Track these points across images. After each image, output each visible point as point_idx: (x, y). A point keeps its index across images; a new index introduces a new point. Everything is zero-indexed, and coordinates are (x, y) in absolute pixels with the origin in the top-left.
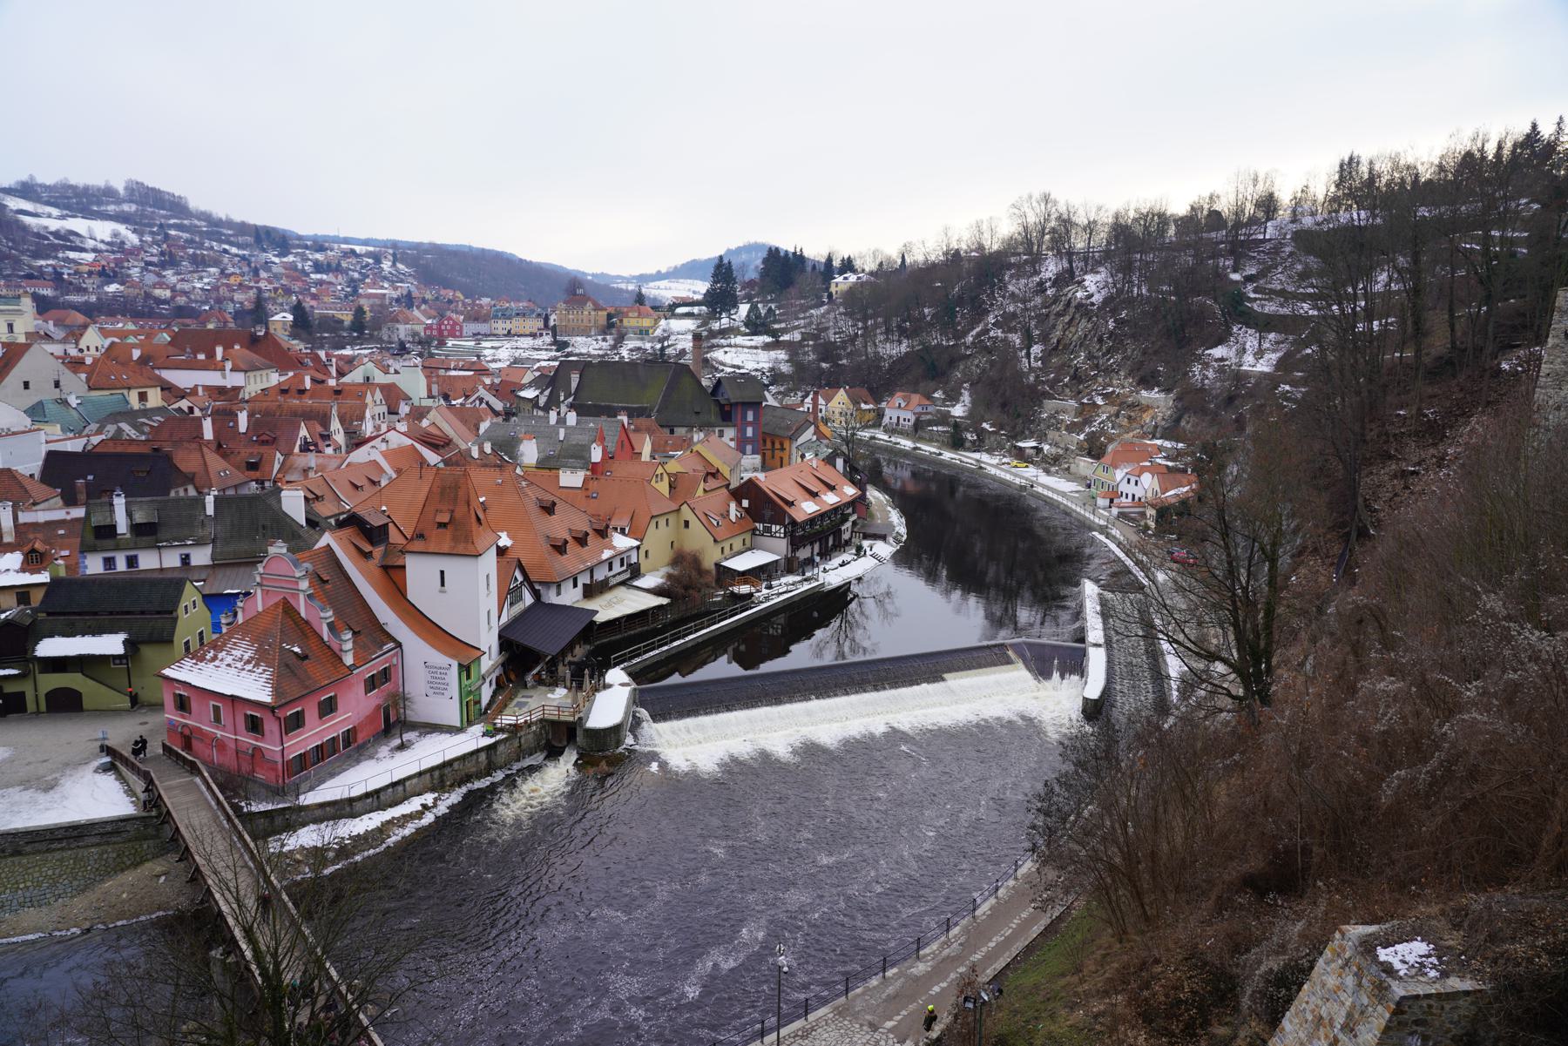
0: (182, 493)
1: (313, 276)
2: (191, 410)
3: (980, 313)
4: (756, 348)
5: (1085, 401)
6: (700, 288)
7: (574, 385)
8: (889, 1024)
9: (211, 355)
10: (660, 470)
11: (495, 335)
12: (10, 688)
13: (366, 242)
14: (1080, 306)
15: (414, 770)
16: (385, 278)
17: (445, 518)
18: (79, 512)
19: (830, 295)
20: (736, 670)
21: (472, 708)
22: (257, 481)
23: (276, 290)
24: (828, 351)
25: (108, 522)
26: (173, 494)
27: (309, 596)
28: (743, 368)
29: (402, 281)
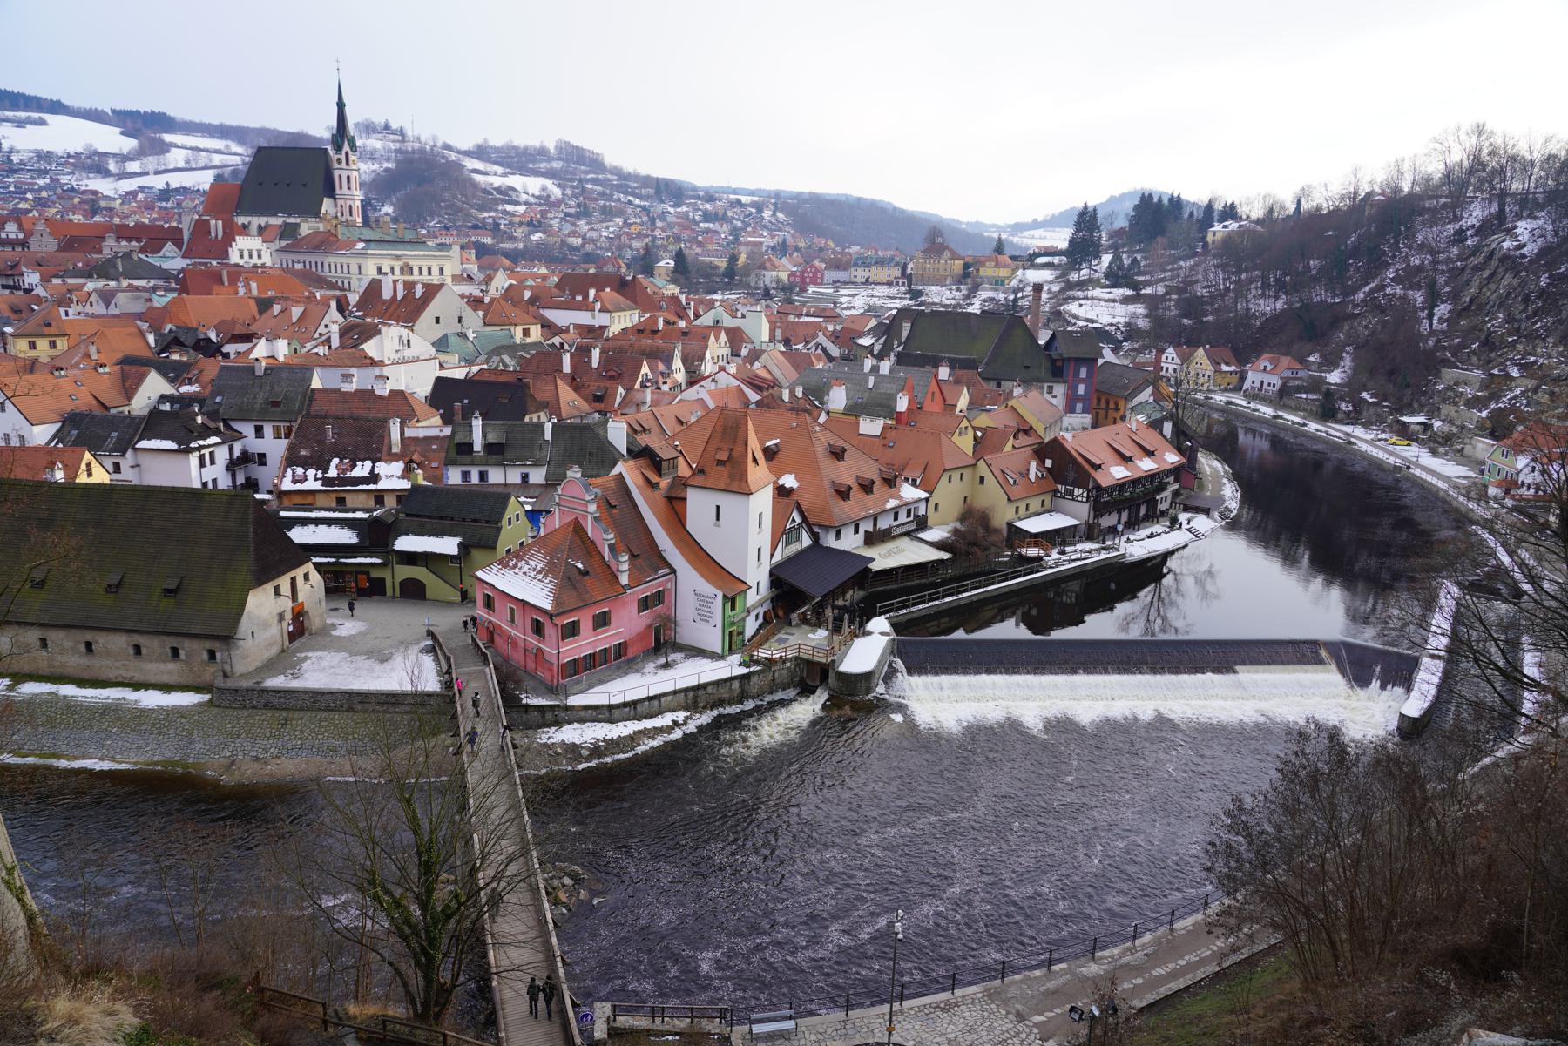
0: (535, 420)
1: (701, 225)
2: (562, 345)
3: (1377, 264)
4: (1114, 301)
5: (1496, 371)
6: (1061, 239)
7: (905, 334)
8: (1038, 1019)
9: (586, 296)
10: (965, 423)
11: (853, 283)
12: (375, 574)
13: (752, 193)
14: (1506, 258)
15: (669, 687)
16: (765, 227)
17: (724, 456)
18: (447, 431)
19: (1205, 245)
20: (1023, 633)
21: (734, 638)
22: (600, 412)
23: (668, 237)
24: (1192, 306)
25: (467, 441)
26: (527, 419)
27: (596, 519)
28: (1097, 322)
29: (780, 230)
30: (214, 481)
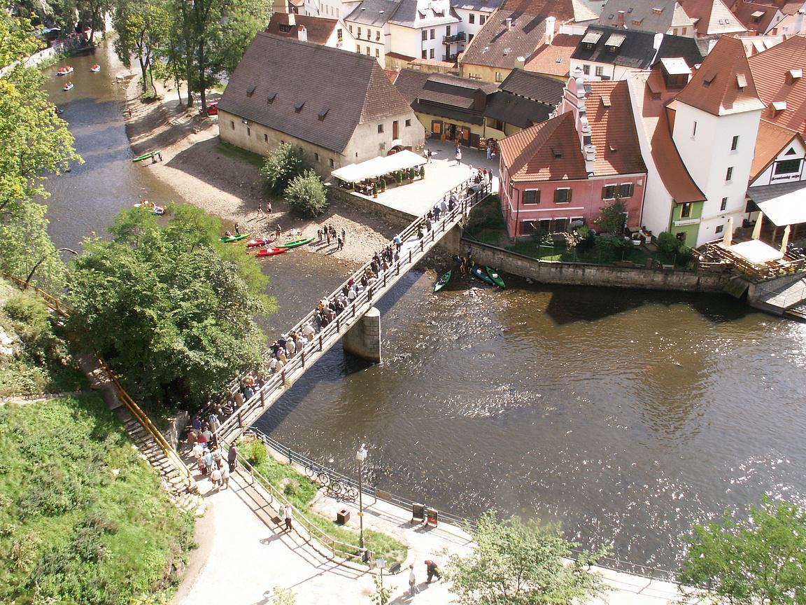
30: (432, 51)
